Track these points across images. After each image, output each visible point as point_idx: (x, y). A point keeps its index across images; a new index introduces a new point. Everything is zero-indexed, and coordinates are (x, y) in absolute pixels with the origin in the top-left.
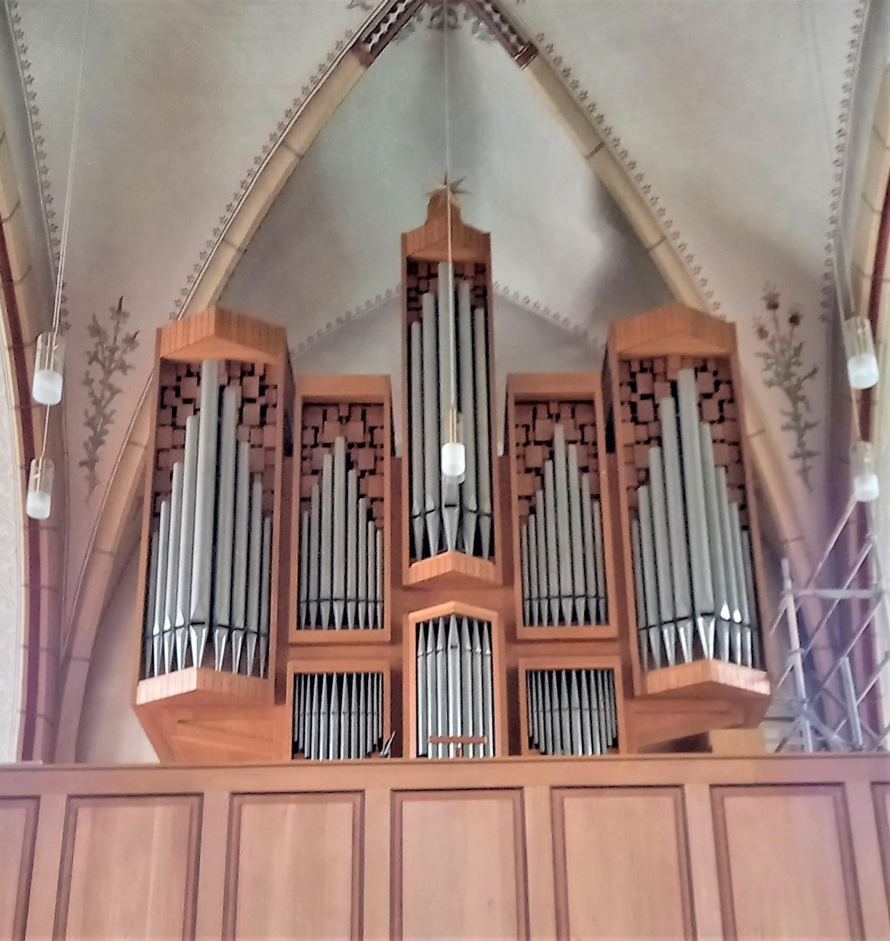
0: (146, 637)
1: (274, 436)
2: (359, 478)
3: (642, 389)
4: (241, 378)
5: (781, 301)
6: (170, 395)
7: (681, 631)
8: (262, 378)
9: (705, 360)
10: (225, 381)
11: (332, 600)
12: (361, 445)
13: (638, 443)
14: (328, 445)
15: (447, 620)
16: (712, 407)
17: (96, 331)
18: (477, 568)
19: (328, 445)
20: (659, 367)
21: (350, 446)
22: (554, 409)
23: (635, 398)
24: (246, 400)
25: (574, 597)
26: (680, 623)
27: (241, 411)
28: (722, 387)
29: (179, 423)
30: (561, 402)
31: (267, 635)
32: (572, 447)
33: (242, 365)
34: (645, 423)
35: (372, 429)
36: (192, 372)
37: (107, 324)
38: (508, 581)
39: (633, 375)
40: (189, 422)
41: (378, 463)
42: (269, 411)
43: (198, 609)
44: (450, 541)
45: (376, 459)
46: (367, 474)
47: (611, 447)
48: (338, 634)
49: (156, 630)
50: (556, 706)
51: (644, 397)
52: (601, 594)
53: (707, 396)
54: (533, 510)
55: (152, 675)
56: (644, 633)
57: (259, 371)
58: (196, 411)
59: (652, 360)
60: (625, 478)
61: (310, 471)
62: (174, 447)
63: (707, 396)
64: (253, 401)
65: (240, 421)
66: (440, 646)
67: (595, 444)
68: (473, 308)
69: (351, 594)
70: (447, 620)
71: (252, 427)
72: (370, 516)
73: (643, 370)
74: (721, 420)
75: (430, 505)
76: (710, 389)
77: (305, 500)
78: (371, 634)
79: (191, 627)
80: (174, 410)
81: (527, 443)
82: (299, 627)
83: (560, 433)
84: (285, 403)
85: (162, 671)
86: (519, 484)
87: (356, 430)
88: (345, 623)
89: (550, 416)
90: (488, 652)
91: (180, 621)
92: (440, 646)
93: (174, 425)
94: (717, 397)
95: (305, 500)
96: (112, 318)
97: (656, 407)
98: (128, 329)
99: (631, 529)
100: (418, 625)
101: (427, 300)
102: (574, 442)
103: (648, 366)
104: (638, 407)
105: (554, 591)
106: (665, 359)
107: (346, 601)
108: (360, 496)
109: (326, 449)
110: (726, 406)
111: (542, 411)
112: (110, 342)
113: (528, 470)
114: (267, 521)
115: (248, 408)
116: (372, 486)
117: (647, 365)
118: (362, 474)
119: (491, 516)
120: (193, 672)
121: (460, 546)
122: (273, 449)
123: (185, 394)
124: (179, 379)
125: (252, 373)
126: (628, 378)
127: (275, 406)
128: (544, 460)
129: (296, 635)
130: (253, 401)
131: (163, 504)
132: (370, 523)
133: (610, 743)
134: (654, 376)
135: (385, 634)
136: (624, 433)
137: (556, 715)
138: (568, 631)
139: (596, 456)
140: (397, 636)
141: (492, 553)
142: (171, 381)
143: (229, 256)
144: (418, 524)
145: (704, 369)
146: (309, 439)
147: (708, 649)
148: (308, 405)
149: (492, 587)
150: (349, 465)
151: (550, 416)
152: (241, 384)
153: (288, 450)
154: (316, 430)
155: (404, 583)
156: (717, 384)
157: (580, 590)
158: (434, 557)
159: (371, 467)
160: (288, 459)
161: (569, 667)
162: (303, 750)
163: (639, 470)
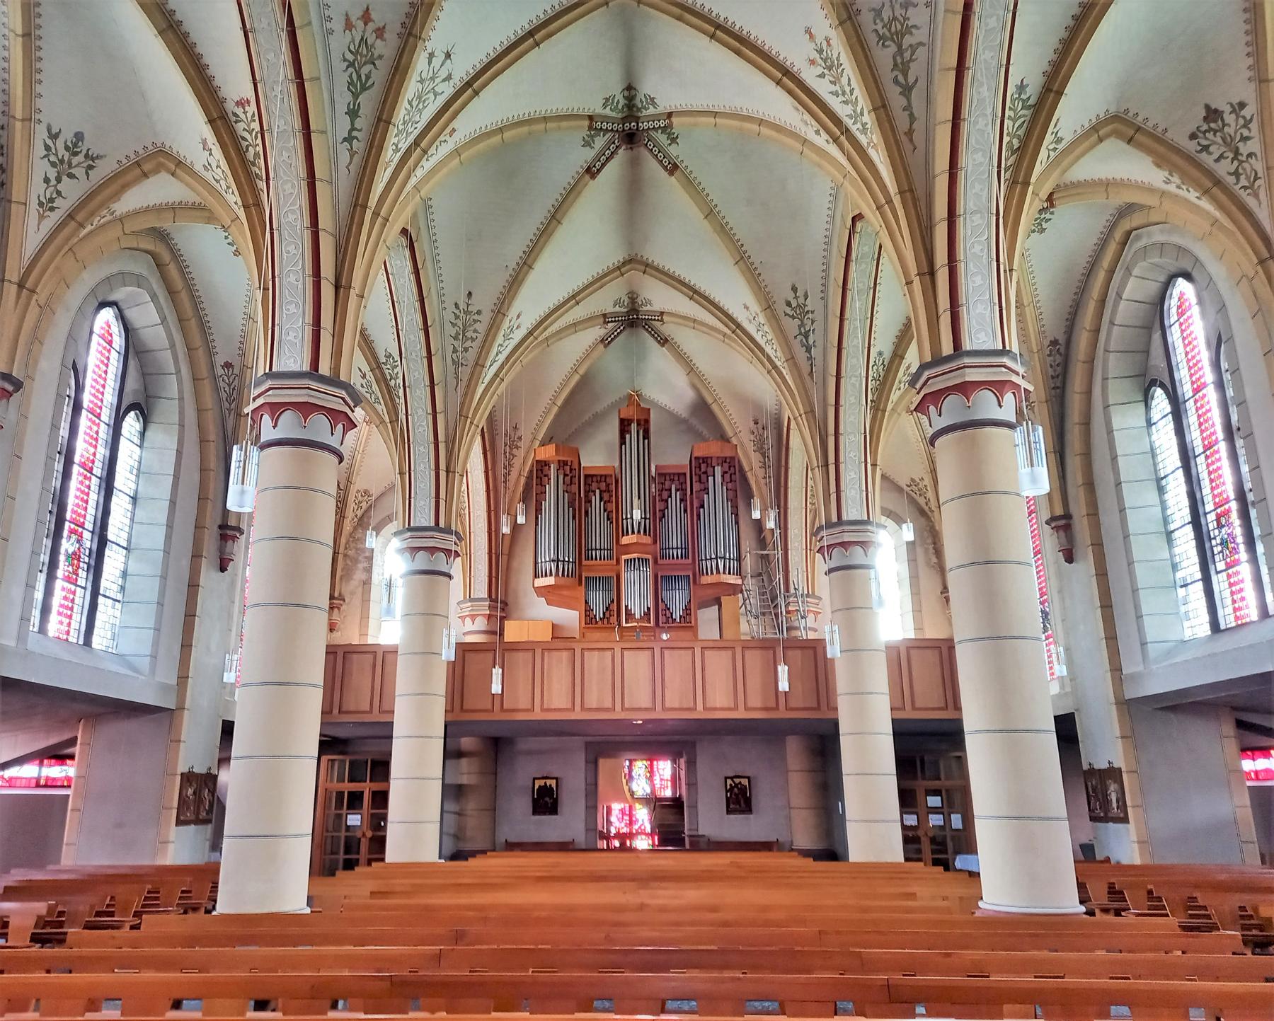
0: (536, 563)
3: (703, 470)
5: (759, 421)
9: (726, 458)
11: (596, 549)
14: (594, 492)
15: (635, 559)
16: (727, 476)
20: (709, 461)
24: (565, 475)
25: (677, 548)
28: (732, 468)
30: (674, 474)
33: (564, 461)
38: (655, 542)
39: (700, 464)
42: (573, 479)
44: (636, 531)
53: (726, 472)
57: (569, 464)
59: (707, 458)
60: (695, 505)
63: (726, 472)
64: (567, 475)
68: (644, 439)
70: (635, 559)
72: (608, 519)
73: (703, 462)
74: (731, 481)
76: (727, 470)
77: (586, 512)
80: (541, 478)
85: (542, 576)
86: (659, 506)
87: (603, 485)
88: (600, 559)
91: (548, 559)
93: (542, 485)
94: (730, 472)
95: (586, 512)
98: (518, 434)
101: (628, 436)
103: (705, 460)
105: (671, 546)
106: (711, 458)
108: (605, 510)
110: (733, 476)
113: (662, 500)
119: (649, 519)
123: (544, 473)
125: (567, 465)
126: (698, 466)
130: (567, 475)
136: (696, 487)
143: (555, 409)
144: (625, 521)
145: (725, 462)
146: (587, 489)
147: (721, 570)
148: (586, 476)
149: (650, 545)
150: (601, 499)
154: (590, 485)
156: (730, 467)
157: (679, 546)
158: (630, 536)
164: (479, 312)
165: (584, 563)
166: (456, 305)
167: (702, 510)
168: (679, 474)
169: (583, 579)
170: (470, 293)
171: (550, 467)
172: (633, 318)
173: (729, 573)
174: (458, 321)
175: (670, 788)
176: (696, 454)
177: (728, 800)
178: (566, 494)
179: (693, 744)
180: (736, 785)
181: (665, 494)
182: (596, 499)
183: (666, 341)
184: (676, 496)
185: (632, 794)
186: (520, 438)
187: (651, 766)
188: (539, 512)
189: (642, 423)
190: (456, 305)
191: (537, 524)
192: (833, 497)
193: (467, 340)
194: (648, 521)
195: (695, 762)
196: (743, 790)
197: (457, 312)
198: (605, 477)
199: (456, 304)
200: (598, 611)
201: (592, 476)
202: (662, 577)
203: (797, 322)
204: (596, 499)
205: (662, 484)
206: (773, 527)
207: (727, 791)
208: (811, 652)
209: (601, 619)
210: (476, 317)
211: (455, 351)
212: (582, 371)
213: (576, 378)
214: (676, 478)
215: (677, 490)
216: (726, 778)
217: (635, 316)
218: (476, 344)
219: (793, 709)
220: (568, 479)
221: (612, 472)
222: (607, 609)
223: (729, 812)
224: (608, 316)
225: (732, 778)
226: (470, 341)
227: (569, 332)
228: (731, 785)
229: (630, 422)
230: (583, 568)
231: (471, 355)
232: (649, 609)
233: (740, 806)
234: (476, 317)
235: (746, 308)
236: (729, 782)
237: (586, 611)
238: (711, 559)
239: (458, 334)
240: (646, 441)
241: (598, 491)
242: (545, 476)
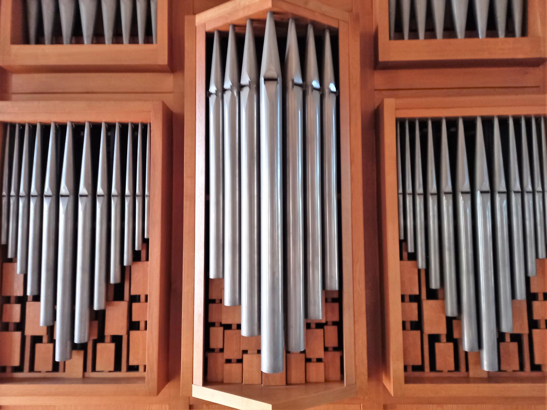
50: (447, 186)
66: (246, 79)
161: (469, 112)
202: (401, 123)
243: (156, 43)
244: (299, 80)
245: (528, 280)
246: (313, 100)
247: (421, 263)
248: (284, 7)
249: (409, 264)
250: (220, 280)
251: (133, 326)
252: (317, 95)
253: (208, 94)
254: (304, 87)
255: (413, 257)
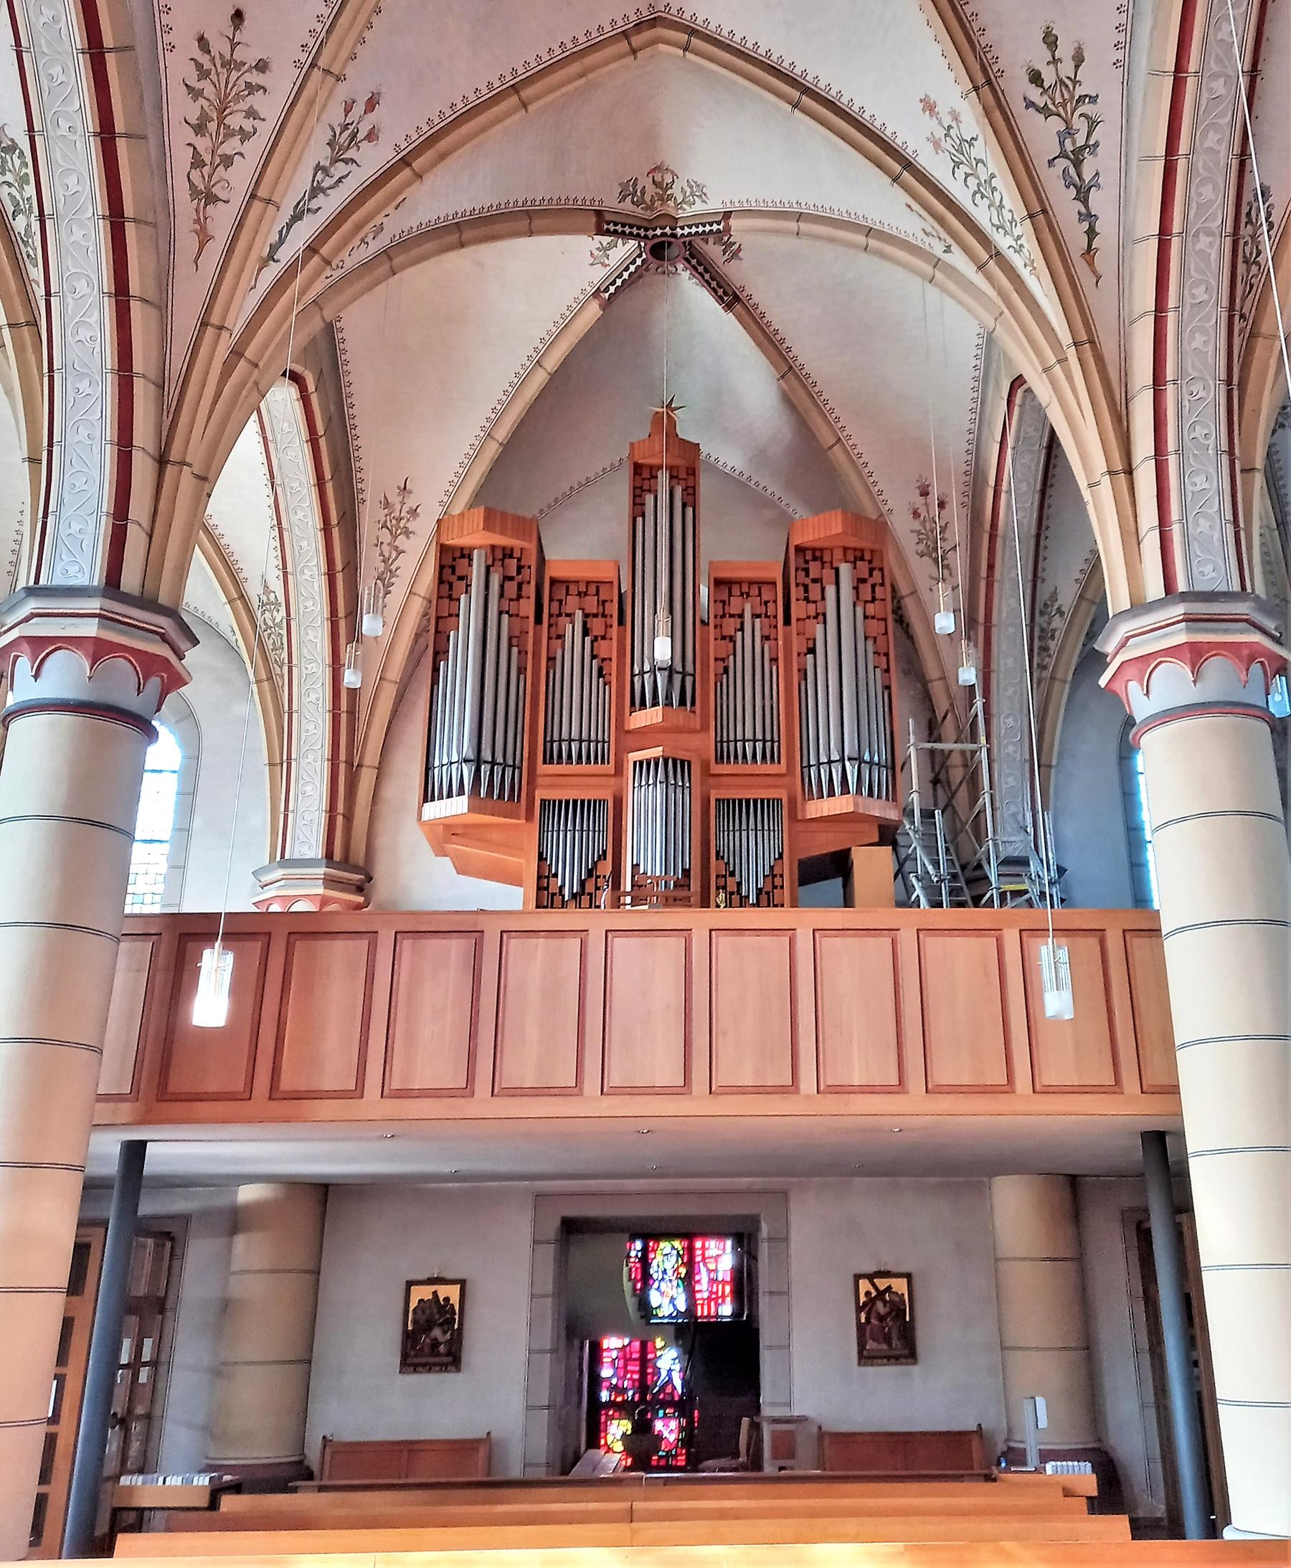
0: (428, 768)
1: (527, 607)
2: (592, 642)
4: (502, 560)
6: (448, 571)
7: (834, 771)
8: (519, 560)
10: (490, 562)
11: (570, 740)
12: (595, 615)
13: (809, 617)
17: (387, 504)
18: (681, 718)
19: (568, 615)
21: (586, 615)
22: (745, 589)
23: (807, 581)
24: (507, 578)
26: (832, 765)
27: (502, 587)
28: (877, 574)
29: (454, 596)
30: (751, 583)
31: (520, 768)
32: (757, 621)
33: (504, 548)
34: (815, 602)
35: (604, 602)
36: (465, 554)
37: (395, 499)
38: (705, 728)
39: (807, 562)
40: (463, 597)
41: (608, 629)
42: (524, 586)
43: (468, 751)
45: (606, 626)
46: (599, 638)
47: (787, 621)
48: (574, 768)
49: (437, 764)
51: (814, 581)
52: (776, 738)
54: (726, 670)
55: (433, 800)
56: (806, 770)
57: (517, 554)
58: (468, 586)
59: (821, 550)
61: (555, 636)
62: (450, 615)
63: (863, 581)
64: (511, 579)
65: (502, 595)
66: (651, 781)
67: (775, 617)
69: (584, 736)
71: (511, 600)
72: (600, 674)
73: (815, 559)
74: (874, 600)
75: (647, 668)
77: (551, 659)
78: (600, 768)
79: (463, 764)
81: (723, 616)
82: (545, 762)
83: (748, 608)
84: (537, 579)
85: (441, 798)
87: (591, 604)
89: (742, 595)
90: (688, 785)
92: (651, 781)
93: (450, 597)
95: (551, 659)
96: (399, 494)
97: (823, 590)
98: (411, 502)
99: (799, 685)
100: (635, 763)
101: (649, 499)
102: (759, 616)
104: (810, 588)
107: (581, 741)
108: (593, 657)
109: (568, 619)
111: (736, 590)
112: (396, 514)
113: (723, 638)
114: (522, 676)
115: (508, 584)
116: (604, 649)
117: (818, 554)
118: (595, 639)
119: (694, 675)
120: (465, 799)
121: (668, 703)
122: (528, 618)
123: (458, 573)
124: (454, 559)
125: (511, 556)
127: (529, 583)
128: (736, 630)
129: (542, 768)
130: (511, 579)
131: (442, 663)
132: (601, 679)
133: (777, 856)
134: (823, 563)
135: (610, 768)
136: (797, 609)
137: (737, 834)
138: (749, 768)
139: (776, 627)
140: (619, 770)
141: (693, 704)
142: (448, 561)
146: (555, 611)
148: (554, 581)
150: (586, 632)
151: (742, 595)
152: (503, 565)
153: (538, 620)
154: (560, 601)
155: (626, 729)
157: (759, 736)
159: (603, 634)
160: (538, 626)
162: (546, 859)
163: (808, 639)
164: (262, 66)
165: (542, 768)
166: (202, 42)
167: (810, 657)
168: (760, 583)
169: (537, 803)
170: (238, 16)
171: (471, 560)
172: (664, 235)
173: (871, 794)
174: (206, 85)
175: (728, 1299)
176: (798, 540)
177: (861, 1328)
178: (505, 617)
179: (785, 1194)
180: (881, 1294)
181: (730, 625)
182: (573, 630)
183: (737, 298)
184: (753, 628)
185: (645, 1309)
186: (414, 512)
187: (690, 1250)
188: (441, 656)
189: (683, 475)
190: (202, 42)
191: (435, 681)
192: (1151, 544)
193: (230, 134)
194: (689, 680)
195: (786, 1240)
196: (897, 1309)
197: (204, 60)
198: (598, 585)
199: (201, 39)
200: (568, 880)
201: (566, 583)
202: (718, 800)
203: (1056, 124)
204: (573, 630)
205: (724, 602)
206: (973, 680)
207: (859, 1309)
208: (1092, 943)
209: (574, 896)
210: (255, 78)
211: (197, 162)
212: (552, 363)
213: (541, 378)
214: (755, 591)
215: (755, 616)
216: (857, 1277)
217: (668, 230)
218: (255, 149)
219: (1049, 1091)
220: (511, 588)
221: (609, 575)
222: (590, 873)
223: (865, 1357)
224: (608, 217)
225: (870, 1277)
226: (235, 141)
227: (512, 226)
228: (868, 1293)
229: (653, 471)
230: (540, 781)
231: (239, 178)
232: (686, 873)
233: (889, 1344)
234: (255, 78)
235: (929, 107)
236: (864, 1285)
237: (539, 878)
238: (830, 762)
239: (204, 118)
240: (690, 511)
241: (579, 615)
242: (461, 578)
243: (608, 763)
244: (673, 782)
245: (772, 868)
246: (679, 790)
247: (726, 861)
248: (667, 755)
249: (720, 861)
250: (638, 865)
251: (597, 888)
252: (681, 788)
253: (634, 788)
254: (676, 784)
255: (723, 858)
